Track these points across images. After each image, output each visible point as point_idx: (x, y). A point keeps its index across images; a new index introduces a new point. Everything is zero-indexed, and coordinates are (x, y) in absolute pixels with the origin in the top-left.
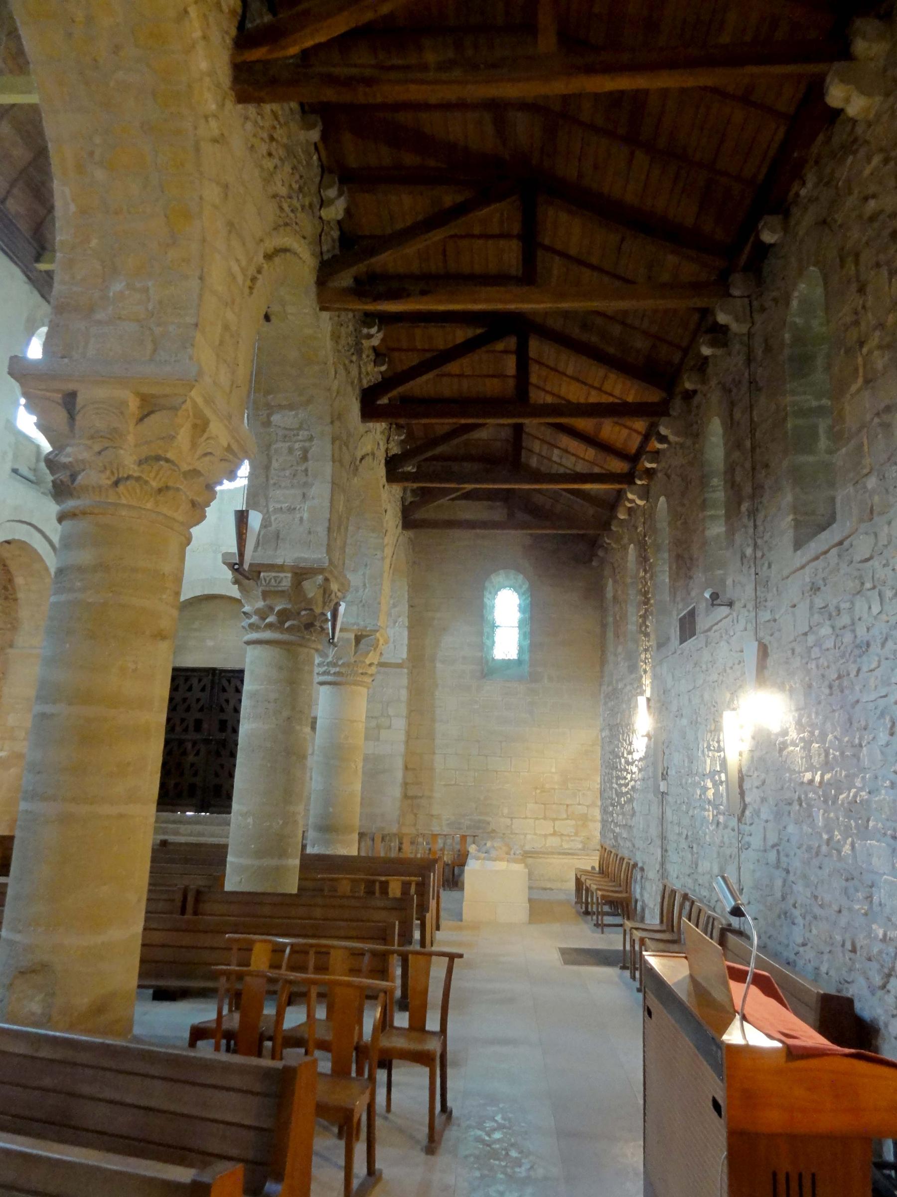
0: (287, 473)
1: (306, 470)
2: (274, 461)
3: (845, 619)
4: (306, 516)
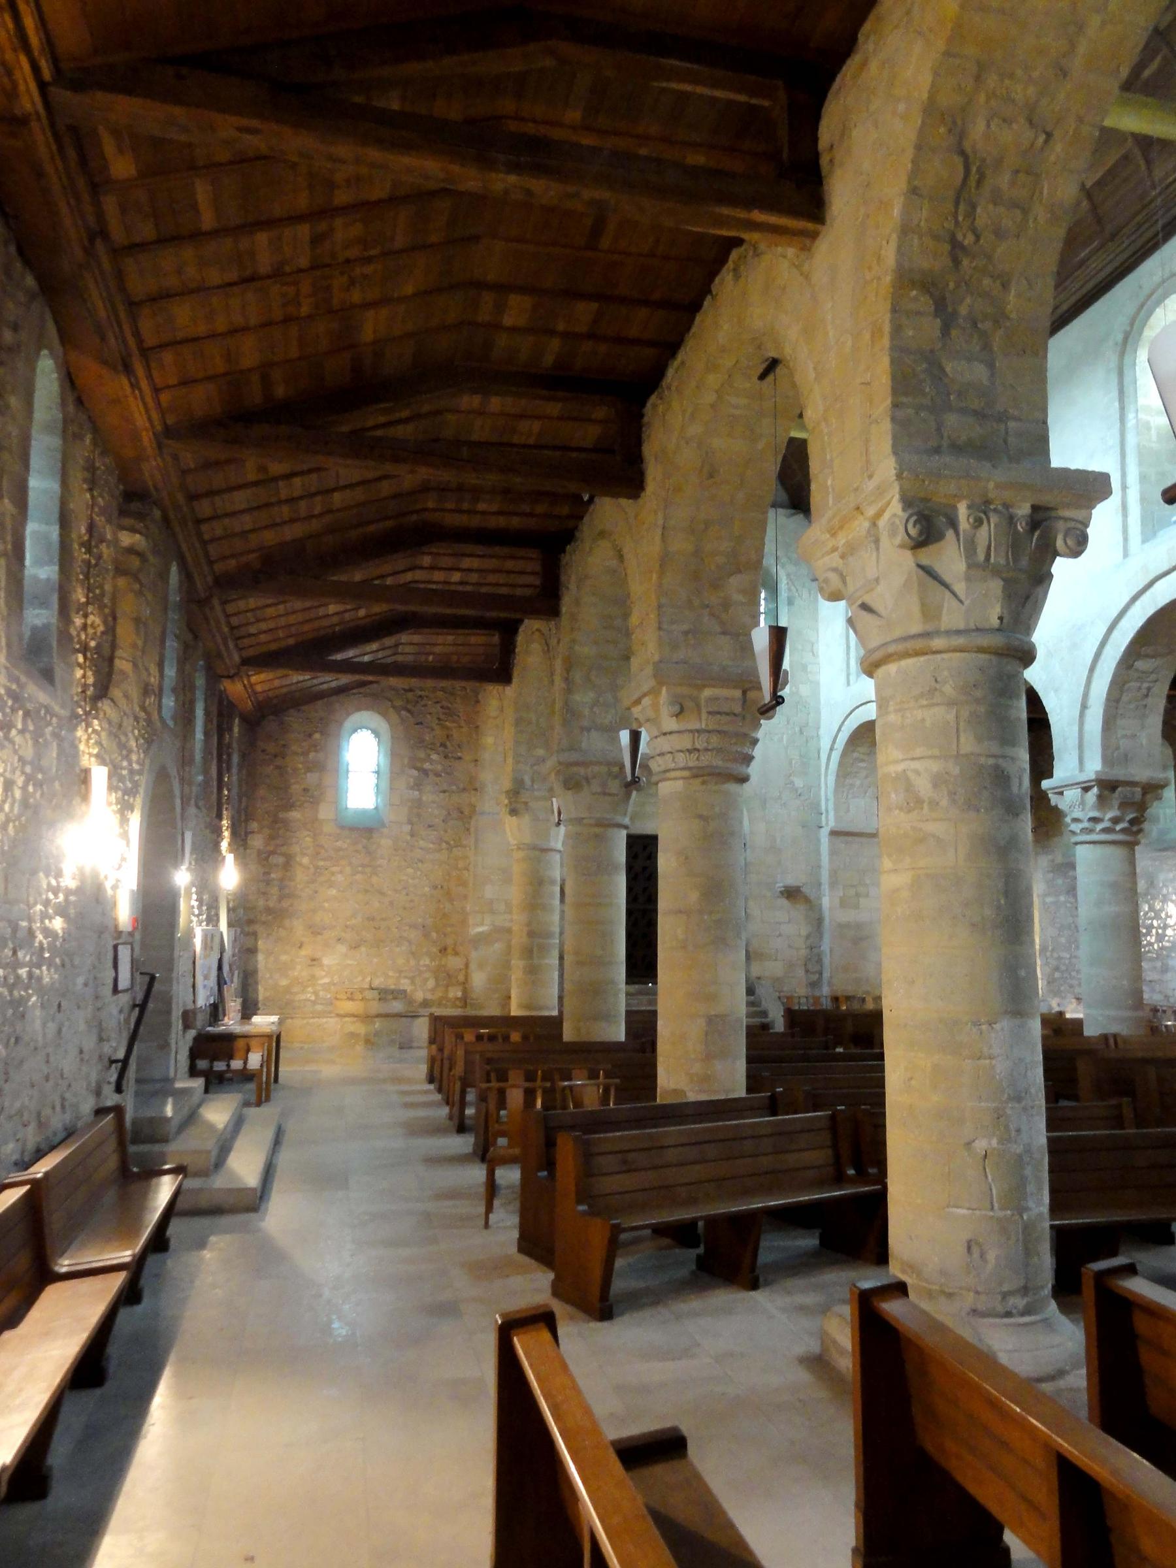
1: (1146, 706)
4: (1144, 742)
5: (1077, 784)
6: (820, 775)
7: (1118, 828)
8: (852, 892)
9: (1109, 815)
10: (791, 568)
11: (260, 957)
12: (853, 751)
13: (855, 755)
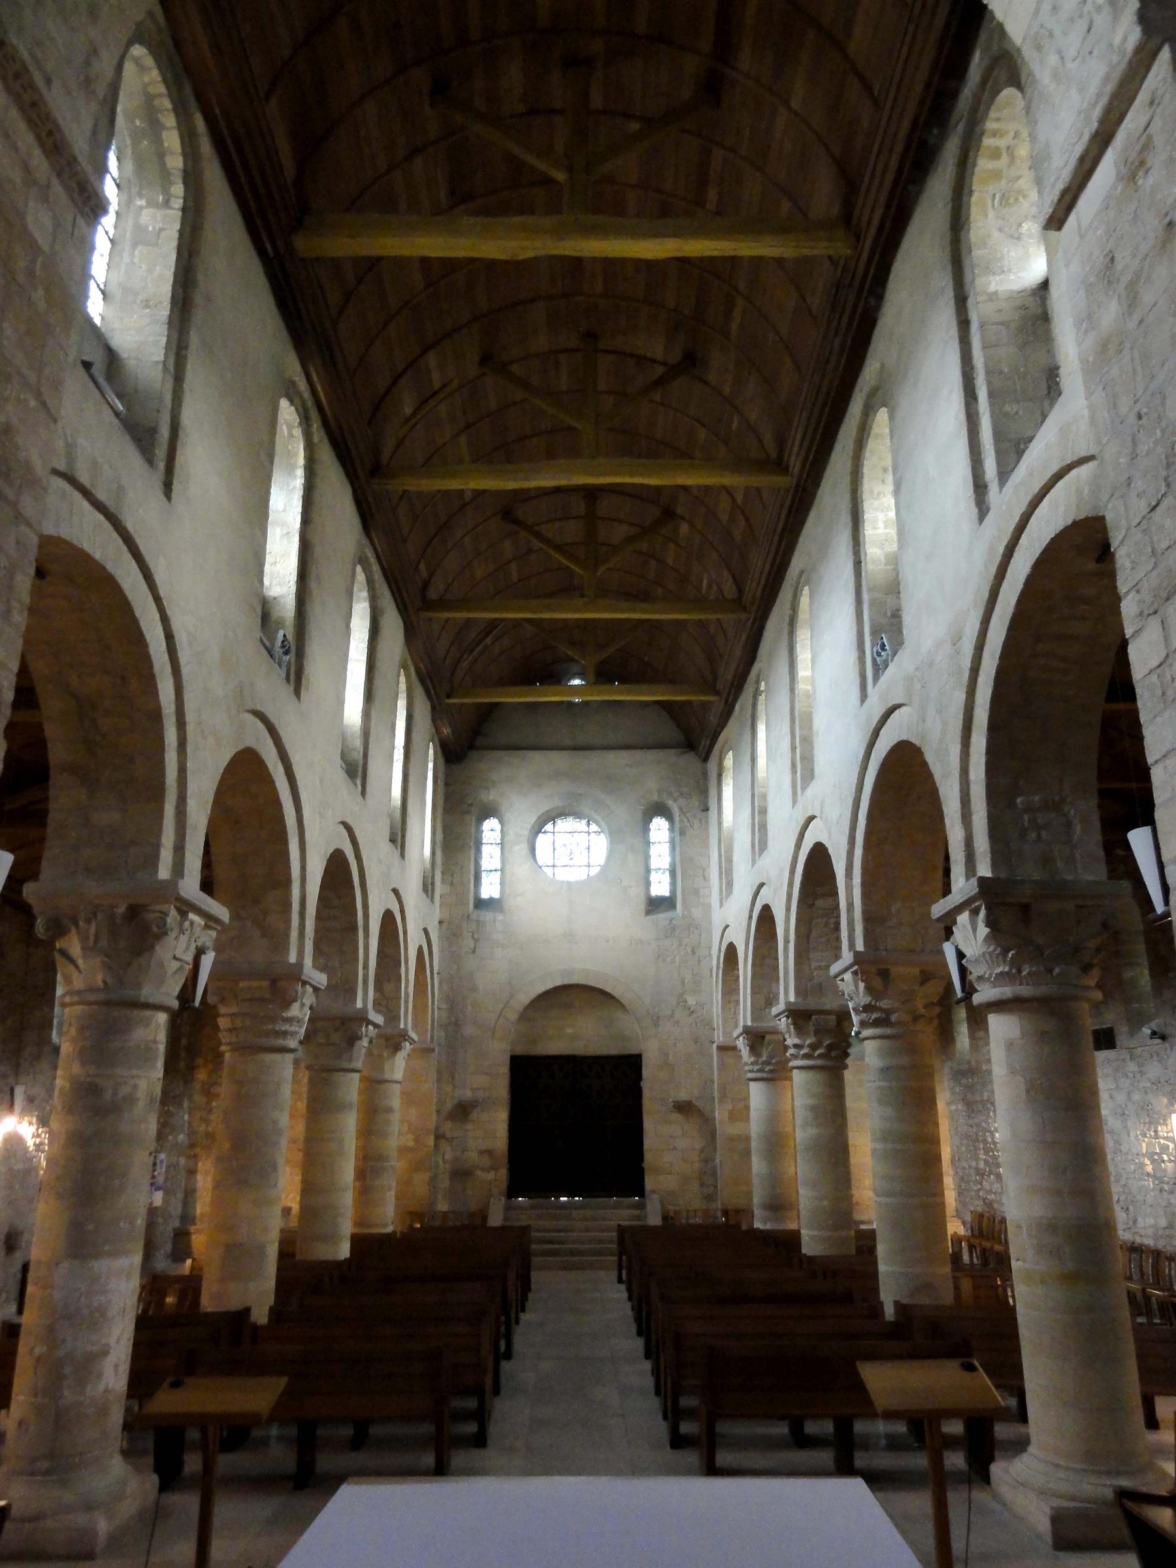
6: (712, 992)
9: (808, 1042)
10: (682, 801)
11: (199, 1177)
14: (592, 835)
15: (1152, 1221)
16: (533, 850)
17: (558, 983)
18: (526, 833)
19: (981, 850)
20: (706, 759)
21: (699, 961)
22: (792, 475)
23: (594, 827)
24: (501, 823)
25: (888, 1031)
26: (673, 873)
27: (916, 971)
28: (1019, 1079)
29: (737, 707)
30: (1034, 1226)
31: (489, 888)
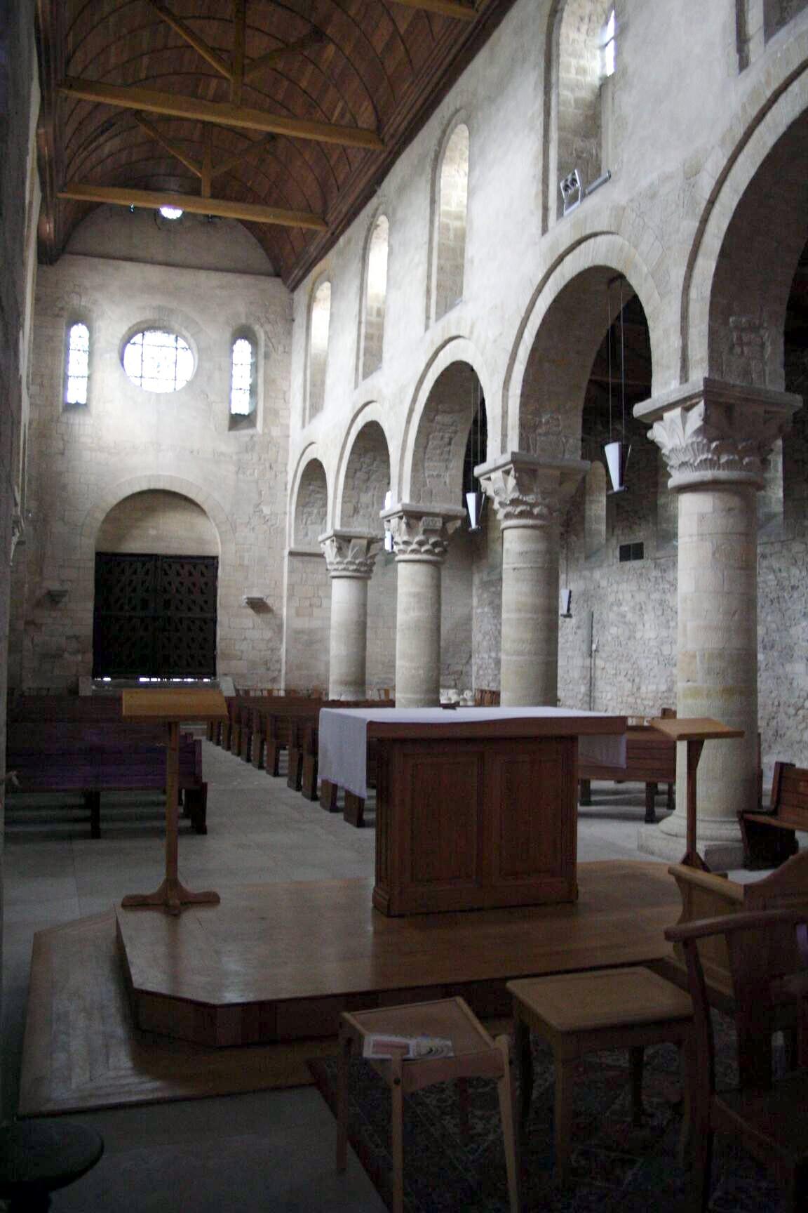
0: (438, 452)
1: (449, 451)
2: (430, 443)
3: (784, 574)
5: (394, 514)
6: (286, 505)
7: (423, 549)
8: (307, 603)
9: (417, 539)
10: (268, 327)
12: (310, 484)
13: (311, 487)
14: (179, 350)
15: (652, 687)
16: (122, 359)
17: (145, 487)
18: (117, 342)
19: (698, 357)
20: (293, 289)
21: (276, 476)
22: (477, 11)
23: (181, 343)
24: (90, 329)
25: (530, 522)
26: (253, 391)
27: (558, 473)
28: (708, 547)
29: (342, 240)
30: (706, 656)
31: (75, 393)
